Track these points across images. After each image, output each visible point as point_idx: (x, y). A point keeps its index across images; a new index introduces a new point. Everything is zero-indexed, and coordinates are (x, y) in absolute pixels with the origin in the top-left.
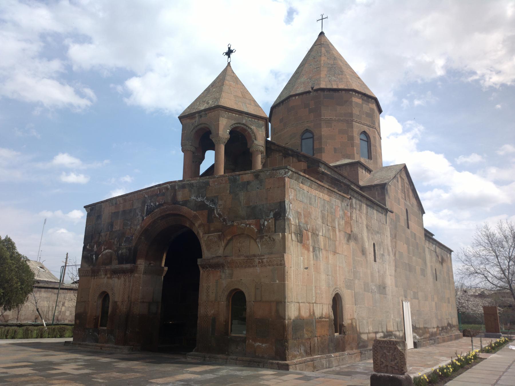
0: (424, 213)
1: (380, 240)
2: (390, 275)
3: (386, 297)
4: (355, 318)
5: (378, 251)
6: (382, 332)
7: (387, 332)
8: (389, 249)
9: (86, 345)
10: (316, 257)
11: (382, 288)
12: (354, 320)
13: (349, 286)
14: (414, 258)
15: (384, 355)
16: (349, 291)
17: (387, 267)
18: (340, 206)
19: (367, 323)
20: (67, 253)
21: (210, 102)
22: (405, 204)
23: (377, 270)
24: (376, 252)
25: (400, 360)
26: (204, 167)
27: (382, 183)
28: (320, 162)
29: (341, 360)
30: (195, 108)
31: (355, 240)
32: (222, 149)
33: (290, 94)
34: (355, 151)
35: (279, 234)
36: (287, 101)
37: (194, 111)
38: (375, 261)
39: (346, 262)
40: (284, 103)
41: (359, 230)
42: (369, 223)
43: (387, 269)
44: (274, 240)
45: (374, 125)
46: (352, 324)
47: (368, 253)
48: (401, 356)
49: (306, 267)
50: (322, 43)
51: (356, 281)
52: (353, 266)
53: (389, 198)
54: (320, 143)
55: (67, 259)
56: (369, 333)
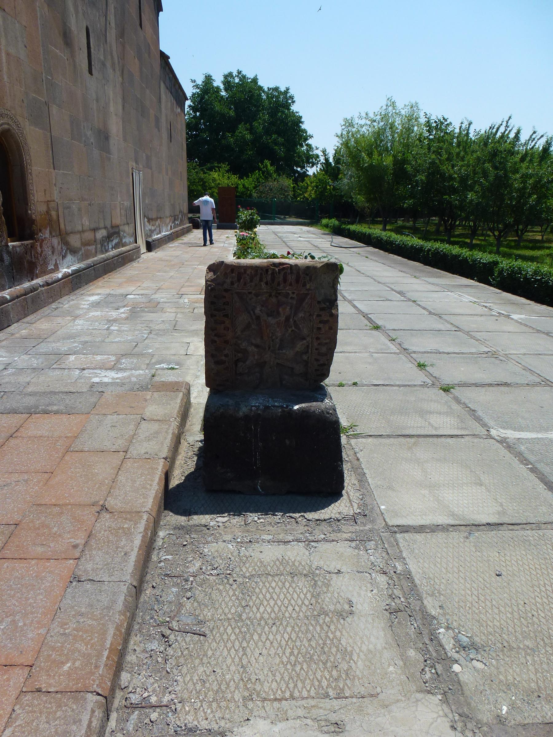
0: (162, 10)
3: (109, 159)
4: (55, 198)
5: (94, 50)
6: (105, 228)
7: (112, 227)
12: (52, 205)
15: (253, 327)
19: (80, 210)
24: (92, 50)
25: (318, 339)
29: (29, 301)
38: (90, 72)
39: (26, 47)
43: (111, 99)
46: (48, 212)
48: (321, 325)
51: (54, 110)
52: (44, 66)
56: (83, 231)
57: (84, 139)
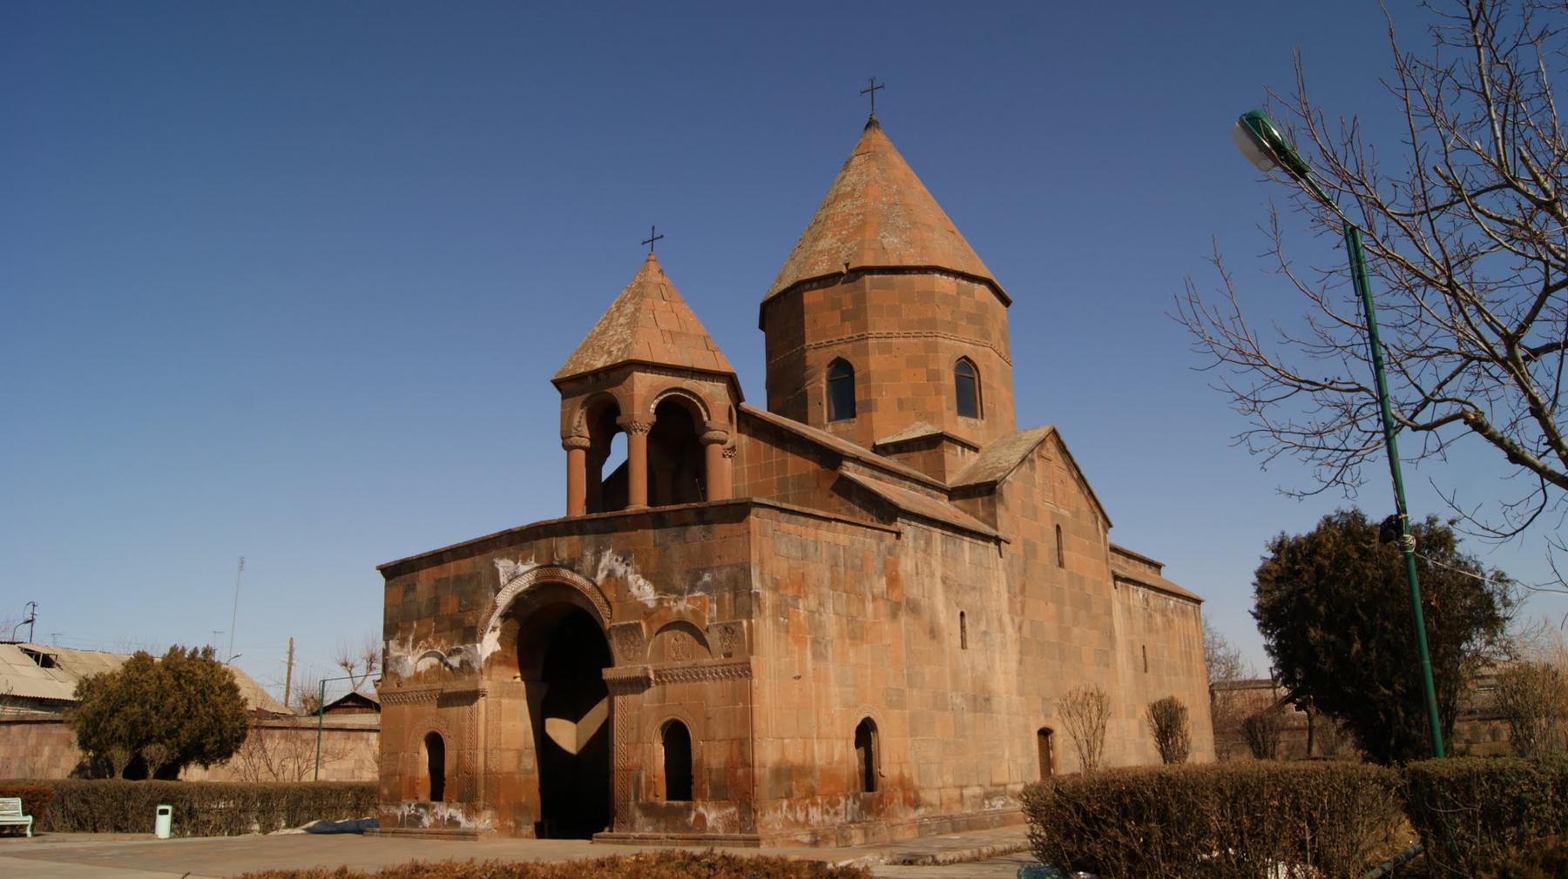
1: (979, 604)
2: (1005, 673)
5: (972, 625)
6: (980, 785)
8: (1004, 618)
9: (406, 832)
10: (817, 655)
11: (982, 701)
13: (896, 701)
14: (1076, 631)
16: (896, 711)
17: (997, 656)
18: (875, 549)
20: (292, 639)
21: (615, 353)
22: (1054, 515)
23: (968, 666)
26: (608, 469)
27: (990, 480)
28: (842, 455)
30: (585, 362)
31: (913, 612)
32: (641, 439)
33: (798, 277)
34: (944, 405)
35: (741, 623)
36: (793, 292)
37: (582, 370)
40: (789, 295)
41: (923, 592)
42: (949, 573)
44: (733, 632)
45: (986, 339)
46: (901, 773)
47: (945, 634)
49: (797, 674)
50: (872, 149)
53: (1007, 509)
54: (868, 389)
55: (291, 653)
57: (950, 707)
